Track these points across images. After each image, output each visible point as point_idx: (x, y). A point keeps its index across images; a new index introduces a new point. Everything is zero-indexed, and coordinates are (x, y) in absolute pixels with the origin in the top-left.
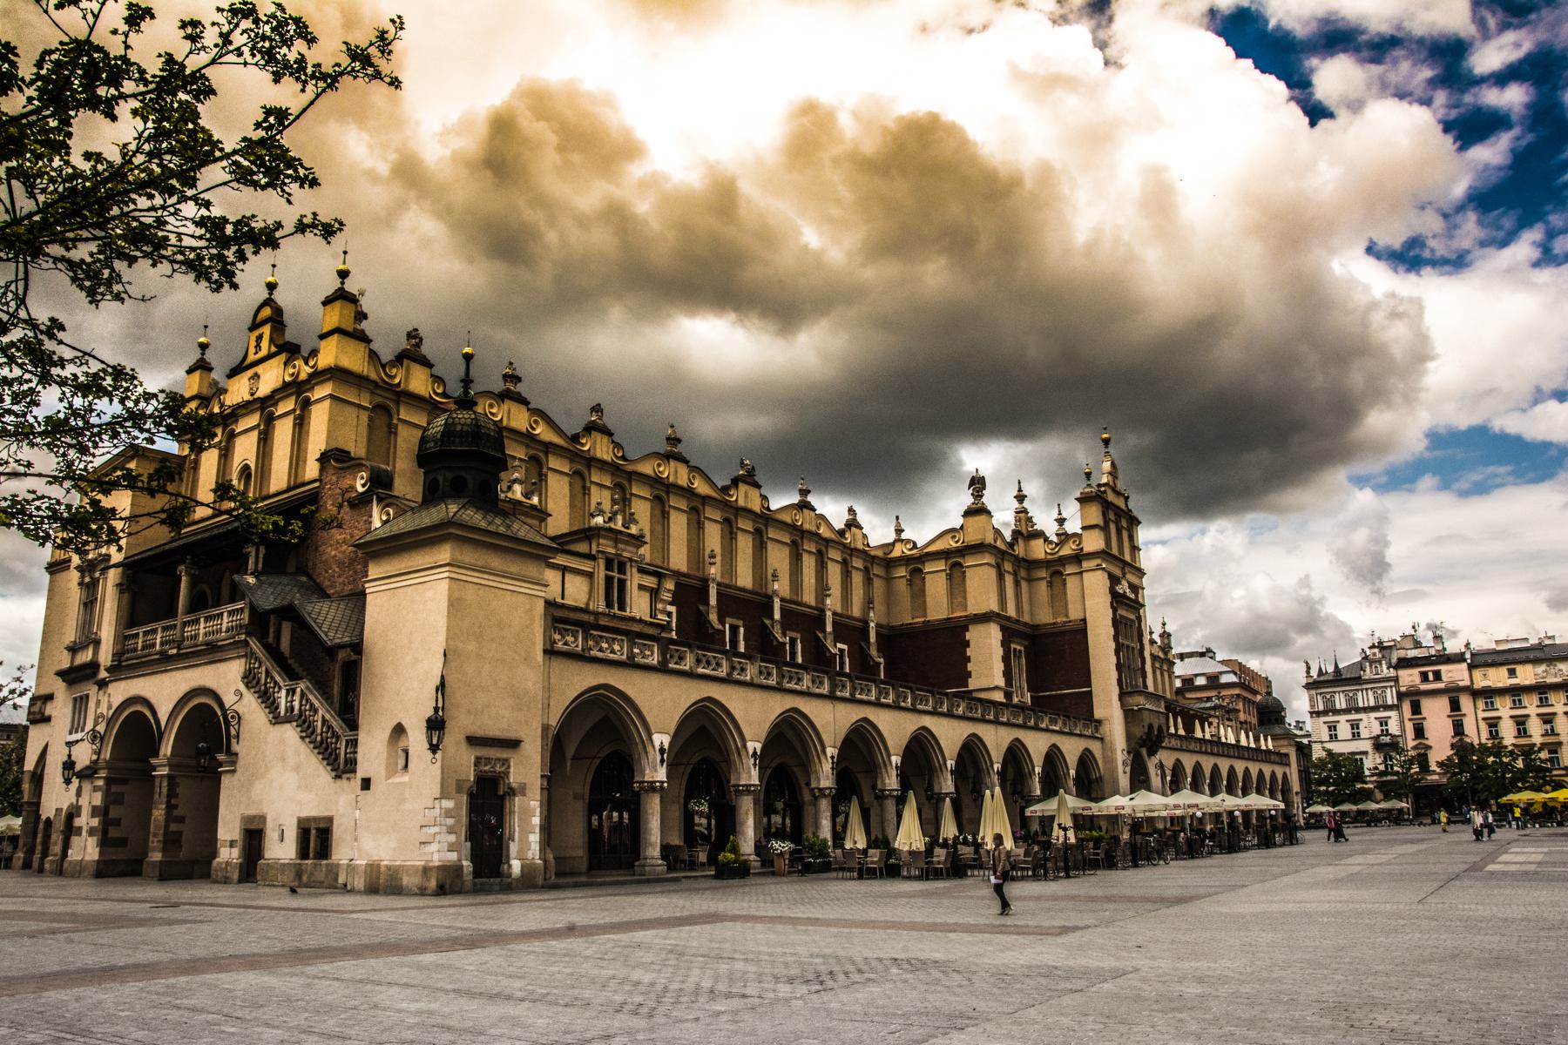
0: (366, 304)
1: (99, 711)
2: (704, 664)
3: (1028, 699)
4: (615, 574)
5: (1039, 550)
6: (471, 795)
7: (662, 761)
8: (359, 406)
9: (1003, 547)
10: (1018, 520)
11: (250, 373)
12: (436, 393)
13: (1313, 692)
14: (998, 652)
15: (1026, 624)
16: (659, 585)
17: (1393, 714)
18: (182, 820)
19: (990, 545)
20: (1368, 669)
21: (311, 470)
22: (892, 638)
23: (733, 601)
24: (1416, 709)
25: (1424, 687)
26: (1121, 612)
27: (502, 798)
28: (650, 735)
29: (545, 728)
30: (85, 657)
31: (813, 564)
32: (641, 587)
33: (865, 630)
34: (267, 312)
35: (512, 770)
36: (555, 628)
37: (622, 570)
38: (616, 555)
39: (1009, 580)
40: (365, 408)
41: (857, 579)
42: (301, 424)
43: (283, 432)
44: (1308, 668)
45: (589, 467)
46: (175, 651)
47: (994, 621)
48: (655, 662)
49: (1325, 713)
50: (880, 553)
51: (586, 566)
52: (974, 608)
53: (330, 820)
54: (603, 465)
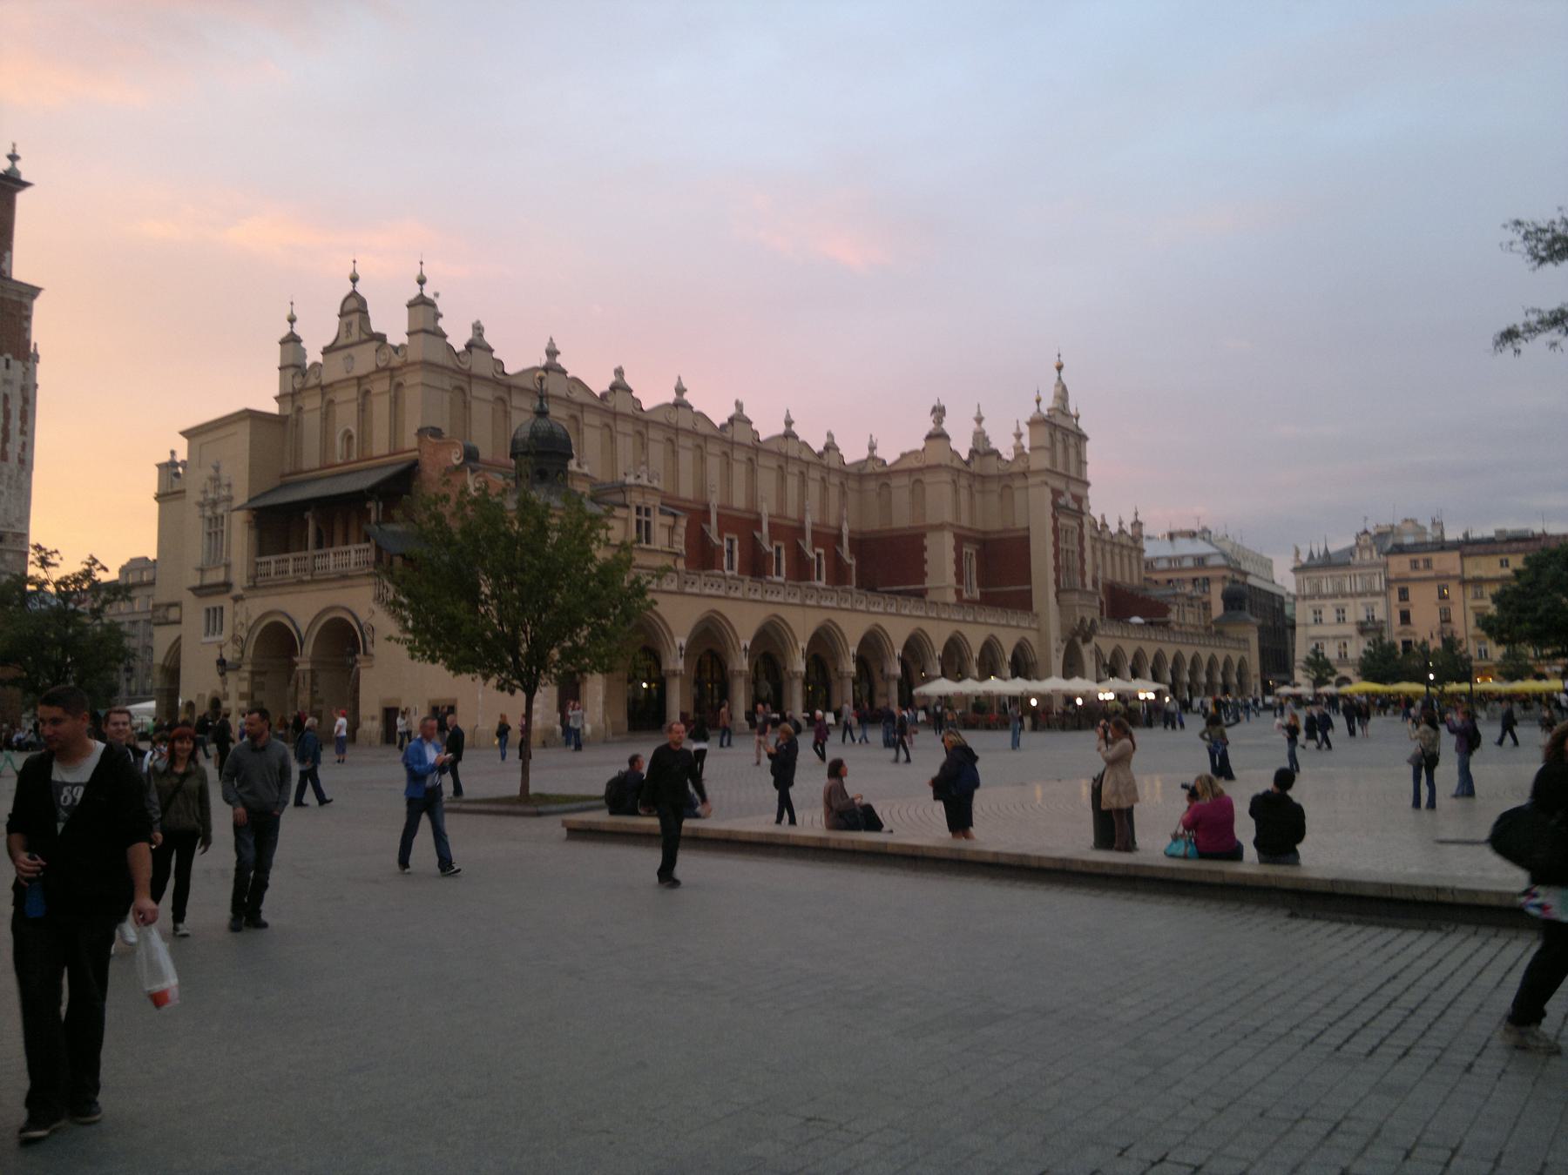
1: (237, 621)
3: (977, 594)
4: (644, 518)
5: (992, 467)
7: (681, 655)
8: (443, 390)
9: (961, 466)
11: (346, 352)
12: (497, 372)
13: (1300, 576)
14: (950, 555)
15: (978, 531)
16: (675, 522)
17: (1381, 600)
18: (321, 701)
19: (947, 466)
20: (1358, 556)
22: (861, 544)
23: (729, 522)
24: (1404, 596)
25: (1415, 574)
26: (1062, 520)
30: (217, 576)
32: (662, 525)
33: (839, 538)
34: (353, 304)
39: (964, 495)
40: (447, 391)
41: (834, 493)
42: (396, 402)
43: (380, 408)
44: (1297, 553)
45: (615, 420)
46: (309, 578)
49: (1312, 597)
50: (854, 470)
52: (931, 519)
53: (456, 700)
54: (625, 416)
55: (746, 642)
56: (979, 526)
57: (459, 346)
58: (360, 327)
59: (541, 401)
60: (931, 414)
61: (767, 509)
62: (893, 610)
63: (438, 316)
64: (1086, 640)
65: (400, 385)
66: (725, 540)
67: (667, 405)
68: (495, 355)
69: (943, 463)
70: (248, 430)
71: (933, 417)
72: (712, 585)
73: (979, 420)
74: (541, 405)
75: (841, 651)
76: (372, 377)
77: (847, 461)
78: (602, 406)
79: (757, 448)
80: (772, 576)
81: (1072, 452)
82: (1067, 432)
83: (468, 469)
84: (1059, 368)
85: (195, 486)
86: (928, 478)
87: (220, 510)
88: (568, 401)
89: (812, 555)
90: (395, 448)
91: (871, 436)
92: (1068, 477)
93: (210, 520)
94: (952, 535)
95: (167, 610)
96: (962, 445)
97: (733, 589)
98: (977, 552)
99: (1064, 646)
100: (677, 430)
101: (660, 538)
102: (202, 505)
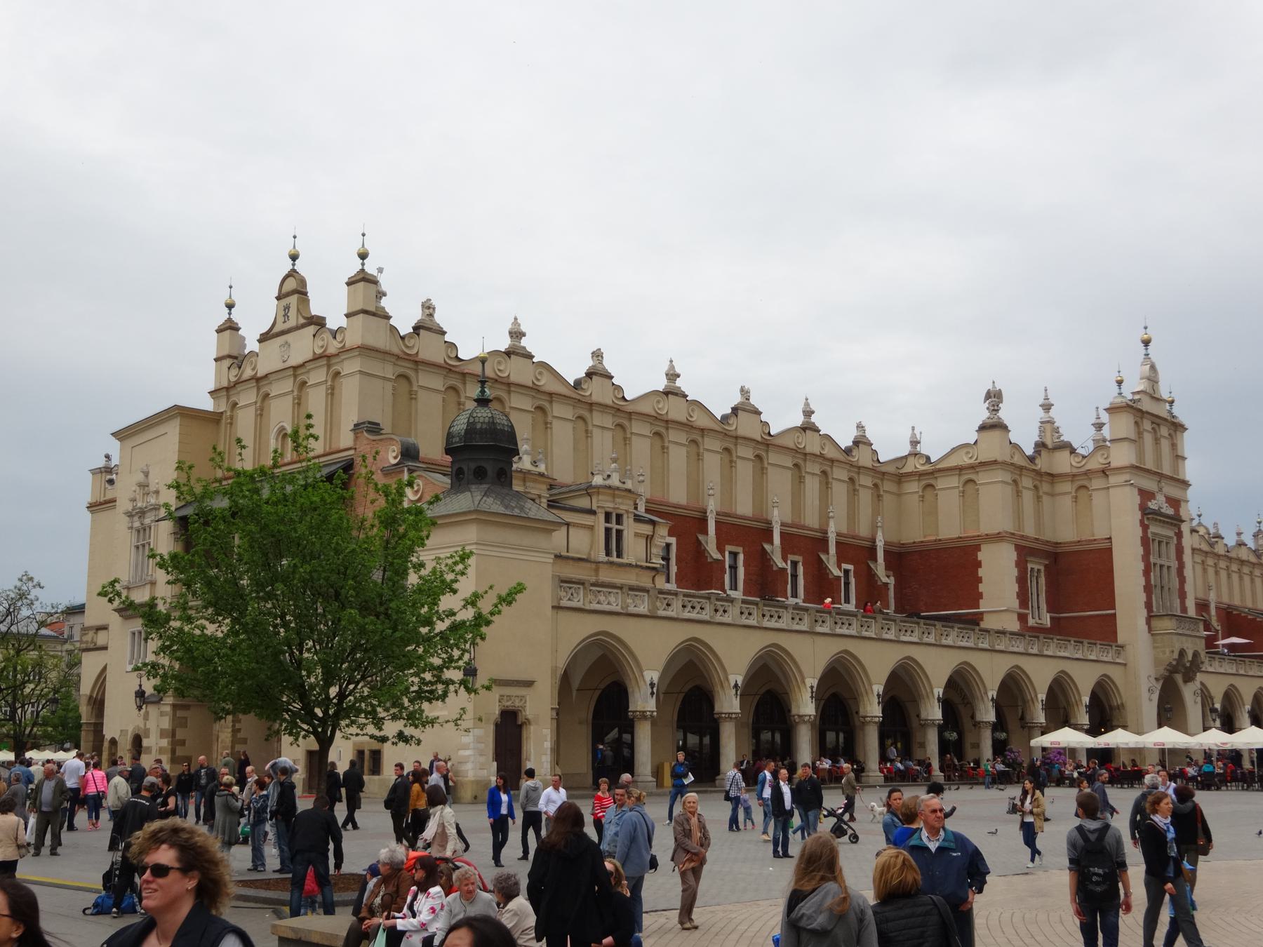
0: (385, 284)
2: (689, 608)
3: (1046, 620)
4: (614, 526)
5: (1063, 463)
6: (497, 725)
7: (652, 693)
8: (384, 378)
10: (1042, 431)
16: (654, 532)
18: (244, 741)
19: (1004, 463)
21: (345, 439)
22: (899, 558)
23: (731, 530)
26: (1153, 529)
27: (520, 727)
28: (641, 671)
29: (554, 670)
31: (817, 486)
32: (637, 535)
33: (873, 550)
34: (291, 284)
35: (528, 704)
36: (561, 587)
37: (619, 519)
38: (614, 508)
39: (1028, 496)
41: (865, 497)
43: (316, 401)
45: (591, 411)
47: (1008, 542)
48: (646, 609)
50: (891, 469)
51: (587, 520)
52: (986, 528)
54: (604, 407)
55: (737, 678)
56: (1048, 536)
57: (405, 328)
58: (298, 310)
59: (483, 387)
60: (985, 402)
61: (778, 517)
62: (931, 639)
63: (381, 294)
64: (1188, 678)
65: (337, 374)
66: (727, 554)
67: (655, 393)
68: (447, 338)
69: (1000, 459)
70: (177, 430)
71: (987, 405)
72: (693, 607)
73: (1047, 407)
74: (483, 392)
75: (863, 689)
76: (309, 366)
77: (883, 458)
78: (574, 395)
79: (766, 443)
80: (787, 598)
81: (1165, 444)
82: (1158, 421)
83: (406, 469)
84: (1146, 343)
85: (125, 491)
86: (982, 478)
87: (147, 521)
88: (534, 390)
89: (836, 572)
90: (330, 448)
91: (913, 428)
92: (1161, 476)
93: (139, 531)
94: (1013, 547)
95: (96, 633)
96: (1025, 435)
97: (721, 612)
98: (1046, 566)
99: (1159, 686)
100: (668, 423)
101: (634, 550)
102: (130, 515)
